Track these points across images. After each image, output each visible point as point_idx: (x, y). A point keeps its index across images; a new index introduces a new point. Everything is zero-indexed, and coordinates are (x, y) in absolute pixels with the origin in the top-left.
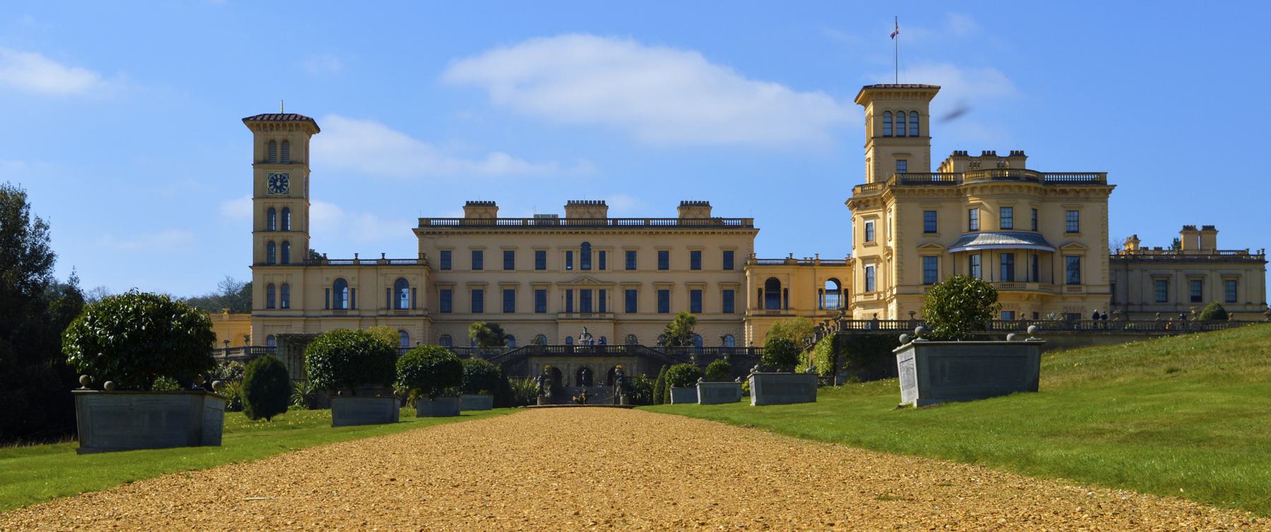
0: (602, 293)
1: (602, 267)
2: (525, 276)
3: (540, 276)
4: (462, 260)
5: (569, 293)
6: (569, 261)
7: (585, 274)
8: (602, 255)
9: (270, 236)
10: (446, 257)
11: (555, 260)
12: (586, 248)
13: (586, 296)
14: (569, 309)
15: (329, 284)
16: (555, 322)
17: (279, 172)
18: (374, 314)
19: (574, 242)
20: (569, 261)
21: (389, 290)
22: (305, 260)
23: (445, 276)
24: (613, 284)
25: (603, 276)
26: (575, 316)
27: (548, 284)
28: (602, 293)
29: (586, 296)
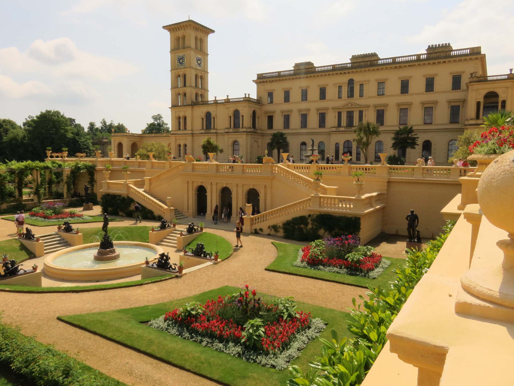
0: (361, 113)
1: (361, 96)
2: (314, 104)
3: (323, 104)
4: (279, 97)
5: (340, 114)
6: (340, 92)
7: (351, 100)
8: (361, 85)
9: (177, 90)
10: (270, 95)
11: (331, 93)
12: (351, 82)
13: (350, 115)
14: (339, 125)
15: (203, 115)
16: (329, 134)
17: (181, 55)
18: (223, 131)
19: (344, 79)
20: (340, 92)
21: (230, 117)
22: (192, 102)
23: (270, 108)
24: (368, 106)
25: (362, 102)
26: (341, 129)
27: (328, 109)
28: (361, 113)
29: (350, 115)
